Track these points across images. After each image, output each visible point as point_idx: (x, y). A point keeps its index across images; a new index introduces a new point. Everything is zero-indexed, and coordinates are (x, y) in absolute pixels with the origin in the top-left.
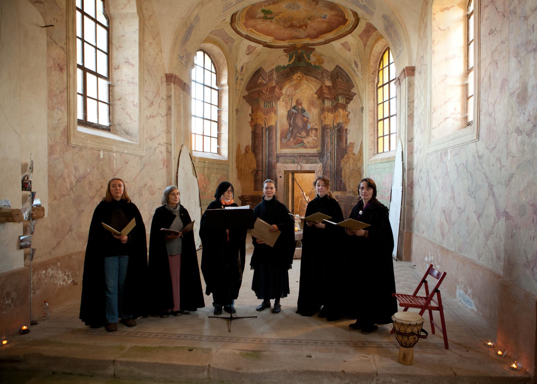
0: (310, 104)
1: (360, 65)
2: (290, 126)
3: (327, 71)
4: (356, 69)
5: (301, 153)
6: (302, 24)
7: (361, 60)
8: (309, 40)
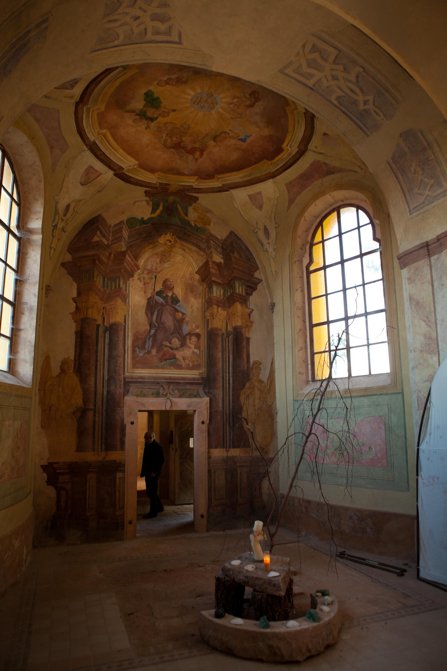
0: (187, 289)
1: (274, 234)
2: (150, 327)
3: (217, 239)
4: (265, 241)
5: (170, 378)
6: (197, 146)
7: (277, 226)
8: (194, 181)
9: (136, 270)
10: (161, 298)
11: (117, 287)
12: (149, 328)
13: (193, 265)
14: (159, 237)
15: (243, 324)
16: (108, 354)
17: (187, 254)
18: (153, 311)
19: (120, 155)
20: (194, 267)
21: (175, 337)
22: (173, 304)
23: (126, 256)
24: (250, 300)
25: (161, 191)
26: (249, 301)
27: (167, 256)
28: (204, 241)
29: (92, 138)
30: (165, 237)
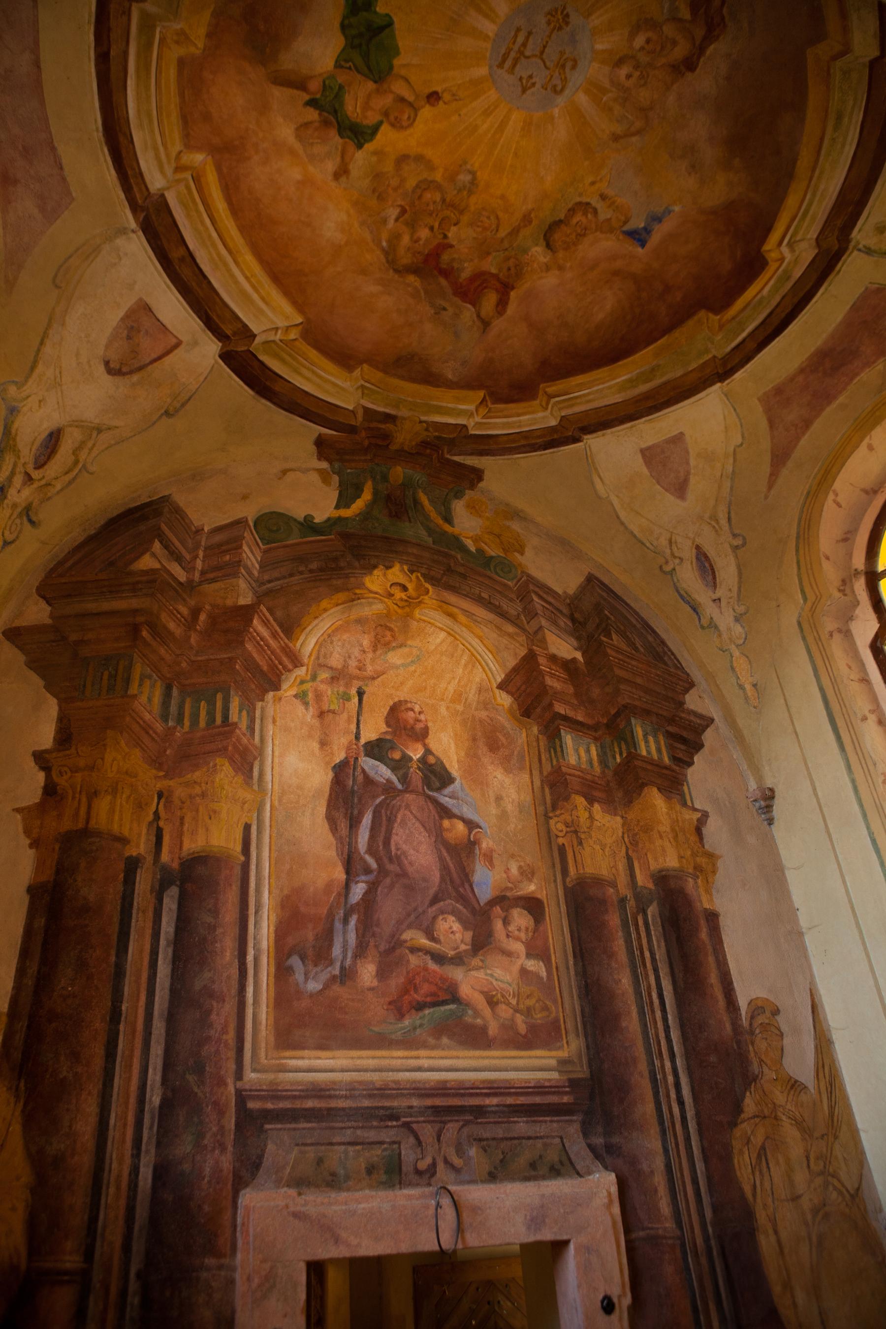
0: (474, 740)
1: (733, 569)
2: (348, 872)
3: (549, 591)
4: (702, 595)
5: (442, 1089)
6: (491, 265)
7: (738, 542)
8: (472, 407)
9: (290, 666)
10: (385, 764)
11: (219, 720)
12: (344, 877)
13: (487, 665)
14: (365, 574)
15: (684, 861)
16: (167, 984)
17: (464, 629)
18: (356, 812)
19: (247, 278)
20: (490, 669)
21: (449, 913)
22: (428, 788)
23: (252, 621)
24: (690, 781)
25: (366, 443)
26: (688, 785)
27: (396, 629)
28: (513, 596)
29: (155, 181)
30: (385, 575)
